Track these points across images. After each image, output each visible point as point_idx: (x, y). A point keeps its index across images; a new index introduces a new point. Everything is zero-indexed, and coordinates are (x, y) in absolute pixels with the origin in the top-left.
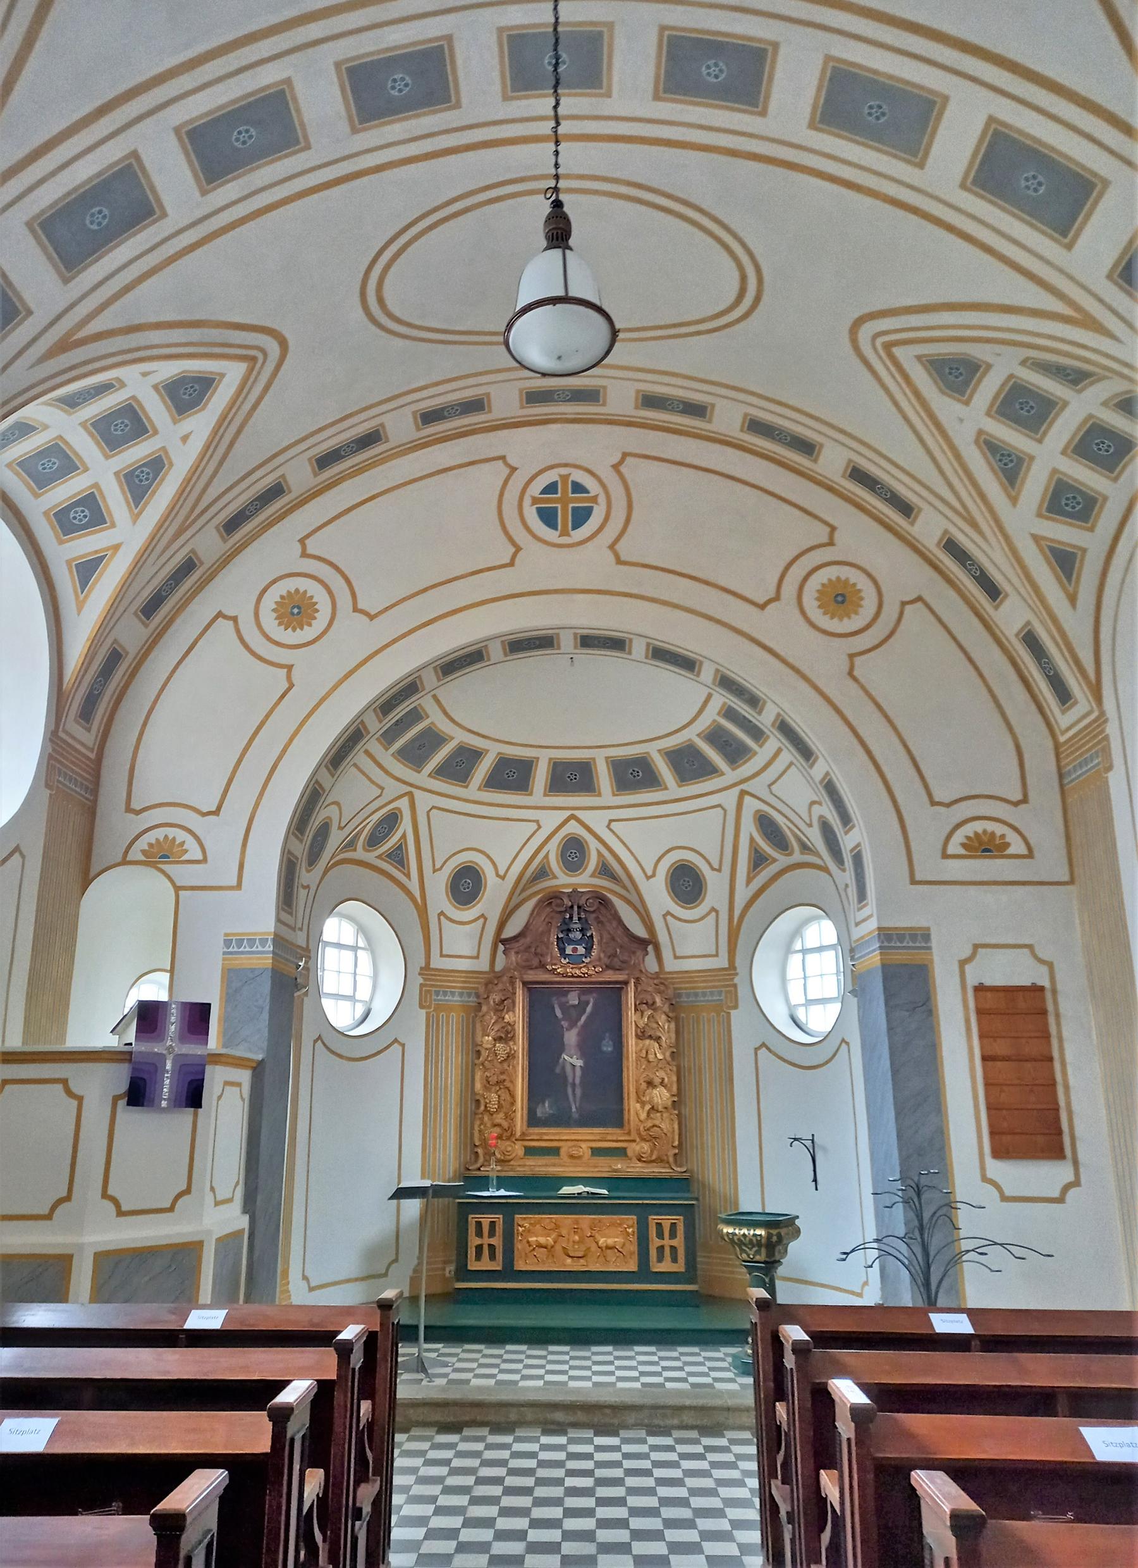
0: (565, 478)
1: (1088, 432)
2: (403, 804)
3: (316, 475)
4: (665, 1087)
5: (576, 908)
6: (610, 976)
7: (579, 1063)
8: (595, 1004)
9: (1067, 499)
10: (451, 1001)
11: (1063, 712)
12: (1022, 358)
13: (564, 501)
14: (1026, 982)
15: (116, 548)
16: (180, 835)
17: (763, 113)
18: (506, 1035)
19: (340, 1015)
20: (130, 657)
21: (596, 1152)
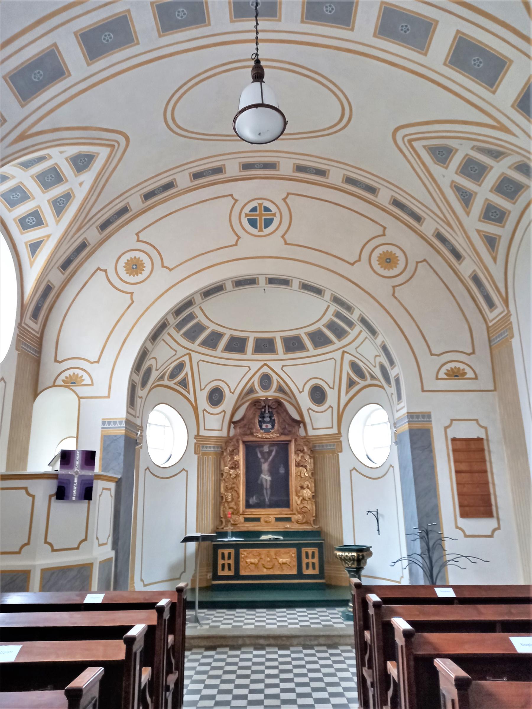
0: (260, 205)
1: (502, 181)
2: (186, 359)
3: (143, 203)
5: (267, 407)
6: (283, 438)
7: (269, 478)
8: (277, 452)
9: (492, 213)
10: (209, 450)
11: (491, 312)
12: (471, 146)
13: (260, 215)
14: (475, 436)
15: (49, 236)
16: (81, 373)
17: (352, 30)
18: (235, 466)
20: (56, 289)
21: (278, 520)
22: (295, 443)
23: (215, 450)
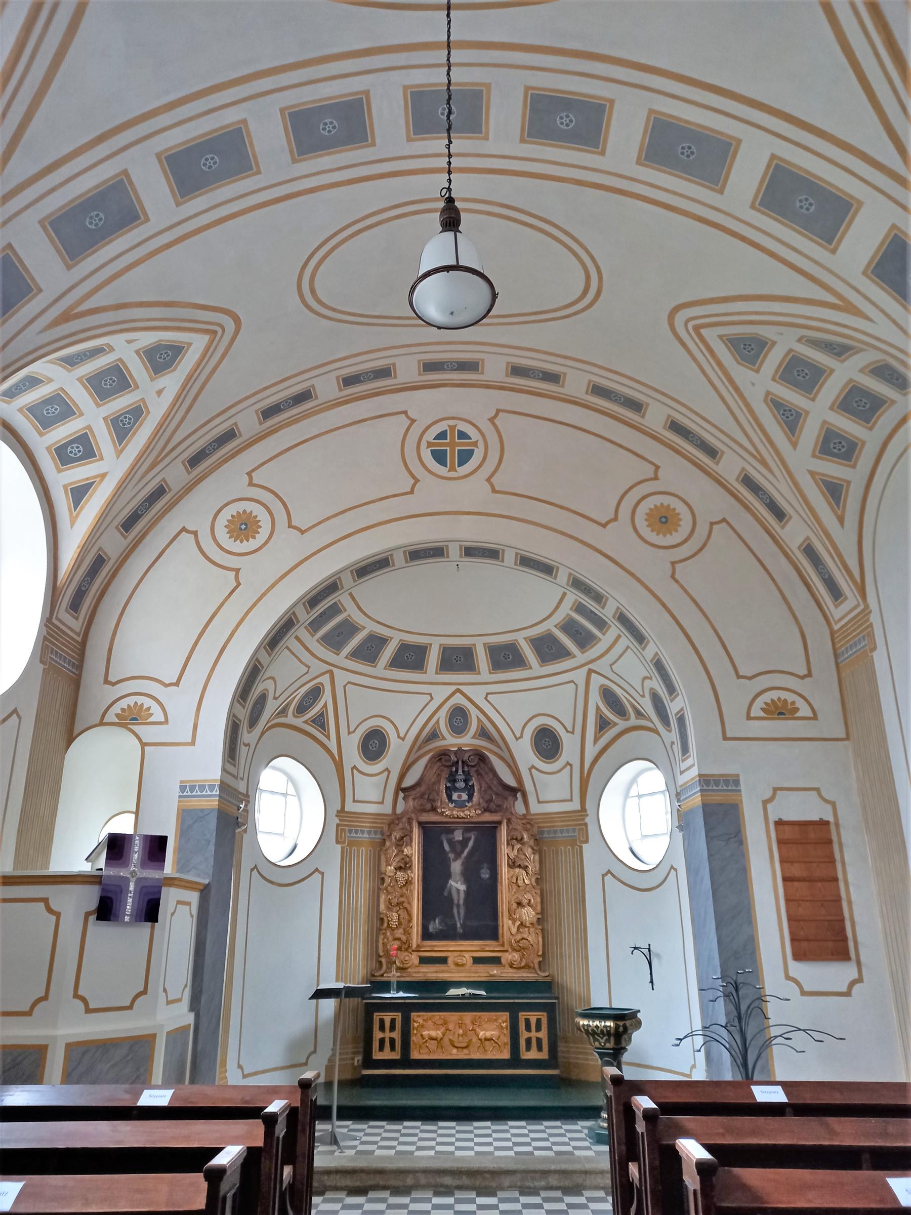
0: (452, 428)
1: (850, 391)
2: (325, 680)
3: (261, 424)
4: (531, 907)
5: (460, 763)
6: (488, 817)
7: (462, 887)
9: (835, 443)
10: (361, 837)
11: (836, 606)
12: (799, 336)
13: (452, 445)
14: (815, 817)
15: (103, 476)
16: (147, 702)
18: (405, 866)
21: (477, 961)
22: (508, 826)
23: (371, 836)
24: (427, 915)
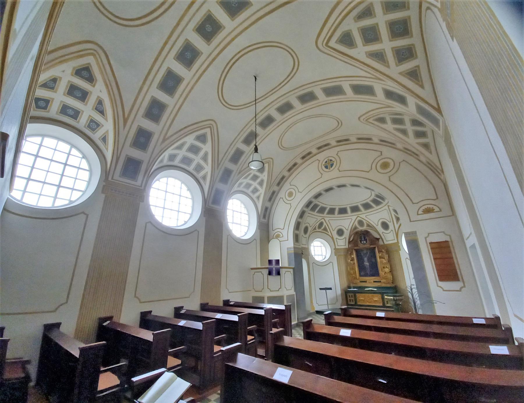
2: (323, 220)
6: (372, 246)
7: (368, 264)
13: (329, 164)
16: (279, 233)
19: (318, 258)
21: (375, 282)
24: (360, 271)
